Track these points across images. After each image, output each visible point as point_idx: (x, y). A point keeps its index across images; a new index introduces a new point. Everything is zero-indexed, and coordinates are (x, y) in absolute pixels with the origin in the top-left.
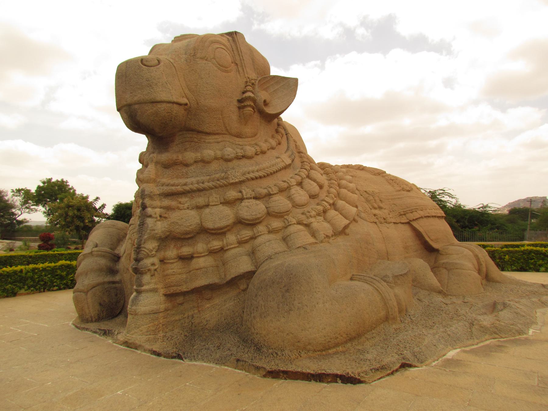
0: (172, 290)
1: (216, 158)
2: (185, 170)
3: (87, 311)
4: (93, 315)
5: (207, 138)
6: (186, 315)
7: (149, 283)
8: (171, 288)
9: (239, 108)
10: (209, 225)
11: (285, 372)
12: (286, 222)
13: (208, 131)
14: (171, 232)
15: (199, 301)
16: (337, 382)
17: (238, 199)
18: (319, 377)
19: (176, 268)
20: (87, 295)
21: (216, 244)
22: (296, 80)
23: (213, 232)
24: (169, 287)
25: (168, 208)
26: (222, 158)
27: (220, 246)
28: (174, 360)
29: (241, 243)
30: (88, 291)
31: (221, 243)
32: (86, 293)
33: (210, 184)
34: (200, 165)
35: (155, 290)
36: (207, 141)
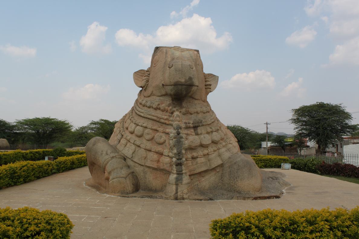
0: (192, 173)
1: (201, 112)
2: (190, 116)
3: (128, 188)
4: (130, 190)
5: (196, 101)
6: (195, 184)
7: (184, 170)
8: (192, 172)
9: (205, 88)
10: (204, 143)
11: (260, 197)
12: (227, 143)
13: (197, 98)
14: (190, 146)
15: (199, 178)
16: (274, 198)
17: (211, 131)
18: (269, 198)
20: (126, 179)
21: (206, 152)
22: (218, 77)
23: (205, 146)
24: (191, 171)
25: (187, 134)
26: (202, 112)
27: (207, 153)
28: (209, 201)
29: (214, 151)
30: (126, 177)
31: (207, 151)
32: (125, 178)
34: (196, 114)
35: (186, 173)
36: (196, 103)
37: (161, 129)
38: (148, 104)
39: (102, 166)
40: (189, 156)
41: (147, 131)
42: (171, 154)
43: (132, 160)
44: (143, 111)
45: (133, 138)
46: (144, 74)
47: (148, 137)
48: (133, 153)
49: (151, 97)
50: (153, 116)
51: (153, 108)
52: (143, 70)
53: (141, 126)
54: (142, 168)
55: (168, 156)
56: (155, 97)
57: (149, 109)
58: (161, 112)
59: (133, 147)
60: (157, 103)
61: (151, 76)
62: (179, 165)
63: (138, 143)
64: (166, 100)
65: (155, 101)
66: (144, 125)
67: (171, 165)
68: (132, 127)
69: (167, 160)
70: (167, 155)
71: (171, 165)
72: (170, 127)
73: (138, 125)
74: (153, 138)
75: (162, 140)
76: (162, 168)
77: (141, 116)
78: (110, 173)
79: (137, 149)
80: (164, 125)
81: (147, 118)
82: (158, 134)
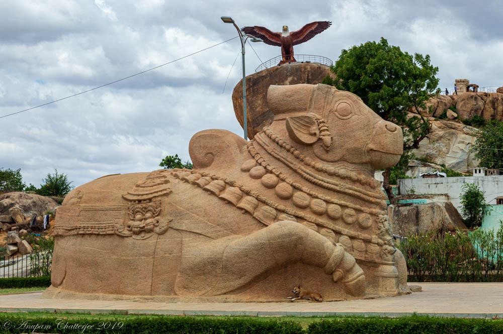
39: (331, 260)
41: (347, 211)
42: (380, 241)
44: (337, 183)
46: (308, 123)
47: (350, 220)
49: (339, 162)
50: (355, 191)
52: (308, 117)
55: (378, 244)
56: (346, 164)
64: (364, 169)
66: (343, 202)
70: (377, 242)
74: (357, 220)
80: (367, 204)
82: (364, 214)
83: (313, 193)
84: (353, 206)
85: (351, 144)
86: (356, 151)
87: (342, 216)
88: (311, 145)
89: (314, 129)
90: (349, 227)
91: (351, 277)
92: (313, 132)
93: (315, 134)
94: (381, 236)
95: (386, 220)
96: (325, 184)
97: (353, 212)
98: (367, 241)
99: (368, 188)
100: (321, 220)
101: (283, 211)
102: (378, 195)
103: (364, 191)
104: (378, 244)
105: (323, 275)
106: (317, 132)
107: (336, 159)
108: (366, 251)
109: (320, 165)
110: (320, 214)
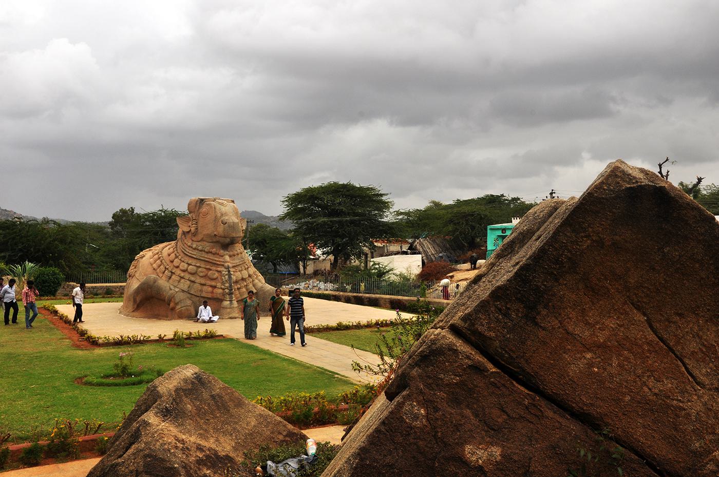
10: (244, 277)
19: (237, 292)
33: (241, 263)
37: (214, 268)
38: (200, 248)
40: (236, 287)
41: (200, 269)
42: (223, 287)
43: (189, 293)
44: (195, 253)
45: (187, 276)
47: (201, 274)
48: (189, 287)
51: (204, 251)
53: (195, 266)
54: (198, 298)
55: (221, 288)
56: (205, 243)
57: (201, 253)
58: (212, 255)
59: (188, 282)
60: (208, 248)
61: (200, 224)
62: (231, 294)
63: (193, 279)
65: (207, 246)
66: (198, 265)
67: (223, 295)
68: (184, 266)
69: (221, 291)
71: (223, 295)
72: (221, 267)
73: (191, 265)
74: (207, 275)
75: (215, 276)
76: (215, 297)
77: (194, 258)
78: (177, 304)
79: (192, 284)
80: (216, 265)
81: (199, 259)
83: (182, 259)
84: (204, 266)
85: (206, 232)
86: (209, 236)
87: (196, 272)
88: (188, 232)
89: (190, 224)
90: (202, 278)
91: (178, 307)
92: (189, 225)
93: (190, 226)
94: (223, 283)
95: (226, 275)
96: (189, 254)
97: (204, 270)
98: (215, 287)
99: (218, 256)
100: (182, 275)
101: (168, 269)
102: (223, 260)
103: (208, 257)
104: (221, 288)
105: (167, 305)
106: (191, 225)
107: (199, 240)
108: (212, 292)
109: (189, 244)
110: (184, 271)
